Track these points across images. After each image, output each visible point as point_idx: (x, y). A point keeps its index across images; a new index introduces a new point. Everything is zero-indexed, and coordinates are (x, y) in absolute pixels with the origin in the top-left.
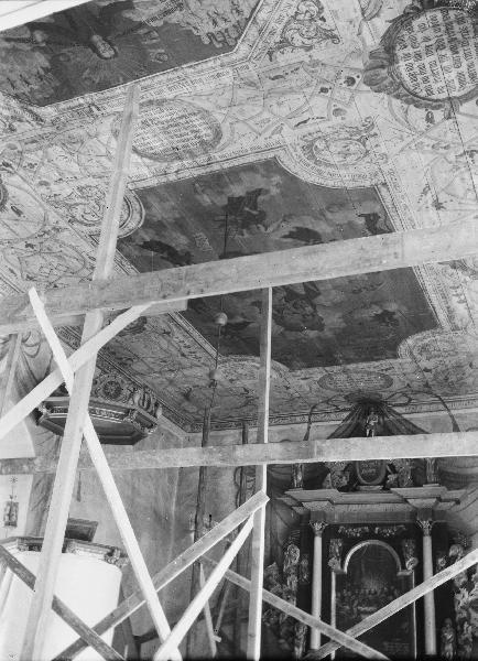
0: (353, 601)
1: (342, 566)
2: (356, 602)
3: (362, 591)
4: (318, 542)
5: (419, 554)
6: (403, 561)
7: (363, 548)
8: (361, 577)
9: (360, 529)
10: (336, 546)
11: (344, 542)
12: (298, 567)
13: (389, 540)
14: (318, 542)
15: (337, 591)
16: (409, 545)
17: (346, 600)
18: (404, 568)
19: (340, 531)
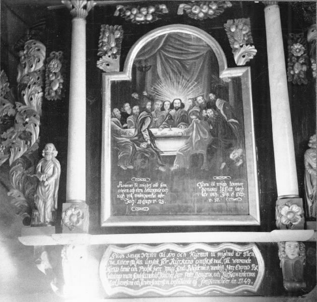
0: (143, 122)
1: (122, 69)
2: (148, 122)
3: (158, 105)
4: (80, 29)
5: (259, 38)
6: (229, 54)
7: (161, 37)
8: (156, 78)
9: (152, 10)
10: (111, 38)
11: (124, 28)
12: (44, 74)
13: (205, 24)
14: (80, 29)
15: (113, 106)
16: (239, 30)
17: (130, 119)
18: (232, 64)
19: (117, 14)
